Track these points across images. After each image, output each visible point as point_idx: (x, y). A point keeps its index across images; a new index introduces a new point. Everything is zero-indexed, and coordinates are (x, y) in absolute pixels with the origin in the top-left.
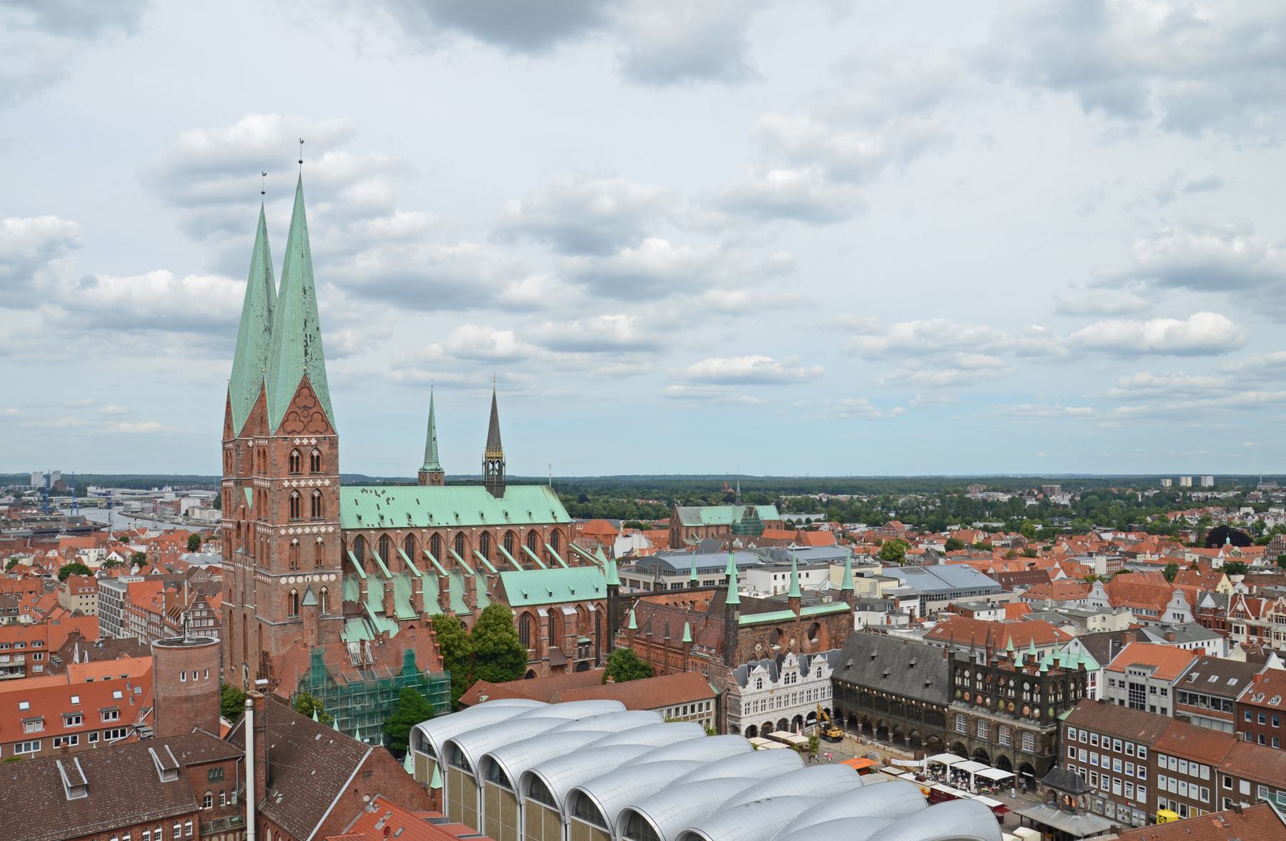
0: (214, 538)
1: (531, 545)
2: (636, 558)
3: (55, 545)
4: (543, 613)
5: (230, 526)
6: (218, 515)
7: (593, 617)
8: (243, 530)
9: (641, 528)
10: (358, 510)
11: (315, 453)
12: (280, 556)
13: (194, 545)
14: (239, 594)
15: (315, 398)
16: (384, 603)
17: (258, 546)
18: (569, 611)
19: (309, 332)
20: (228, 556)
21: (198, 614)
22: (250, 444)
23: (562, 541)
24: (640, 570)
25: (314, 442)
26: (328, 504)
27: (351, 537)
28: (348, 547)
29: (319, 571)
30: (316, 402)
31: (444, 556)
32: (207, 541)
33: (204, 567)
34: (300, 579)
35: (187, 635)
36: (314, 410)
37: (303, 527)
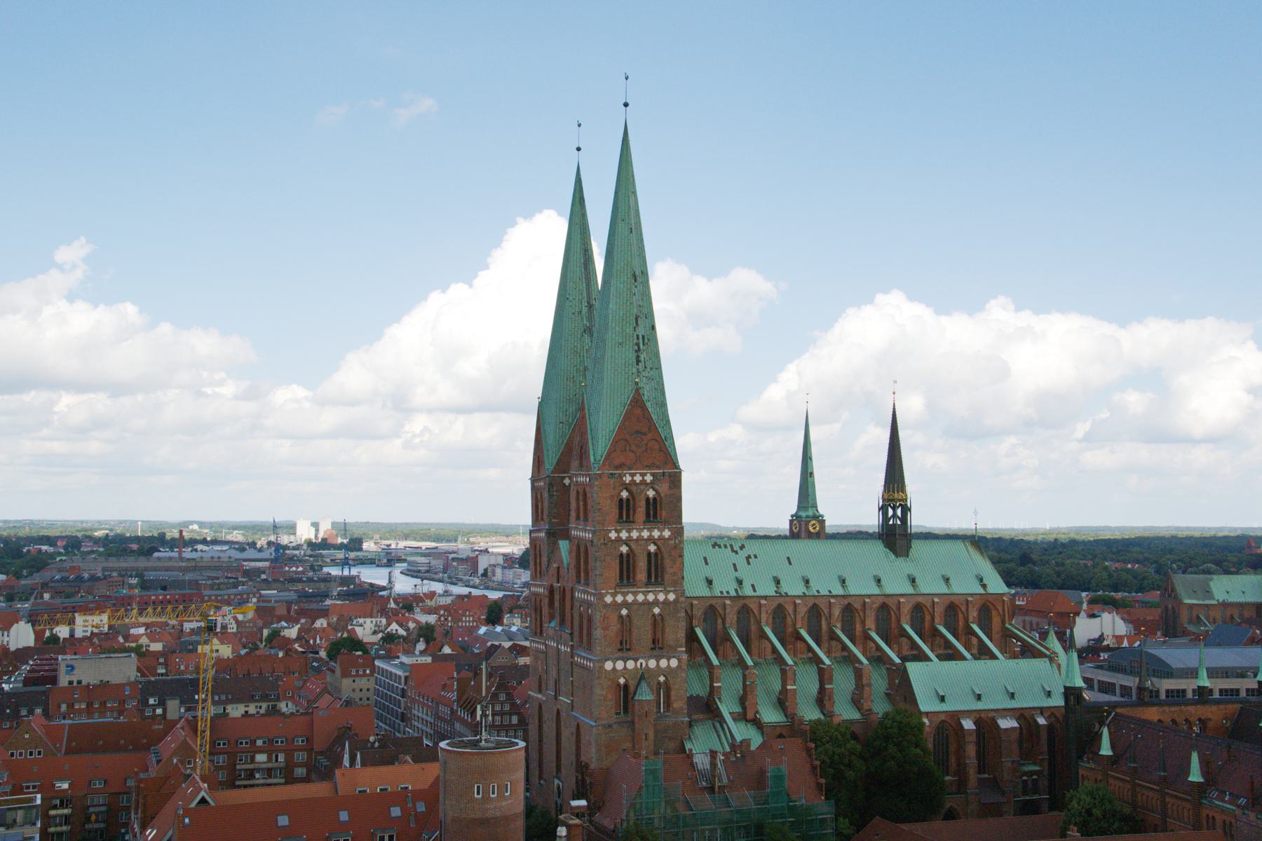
0: (521, 607)
1: (949, 626)
2: (1107, 649)
3: (324, 613)
4: (968, 724)
5: (541, 590)
6: (525, 576)
7: (1044, 735)
8: (557, 597)
9: (1114, 605)
10: (708, 572)
11: (651, 493)
13: (494, 614)
14: (551, 683)
16: (743, 700)
17: (576, 619)
19: (641, 331)
20: (538, 631)
21: (498, 708)
22: (567, 481)
23: (996, 621)
24: (1113, 668)
25: (649, 478)
26: (667, 563)
28: (695, 622)
29: (656, 652)
30: (652, 427)
31: (825, 637)
32: (511, 612)
33: (507, 644)
34: (631, 664)
35: (484, 735)
37: (635, 594)
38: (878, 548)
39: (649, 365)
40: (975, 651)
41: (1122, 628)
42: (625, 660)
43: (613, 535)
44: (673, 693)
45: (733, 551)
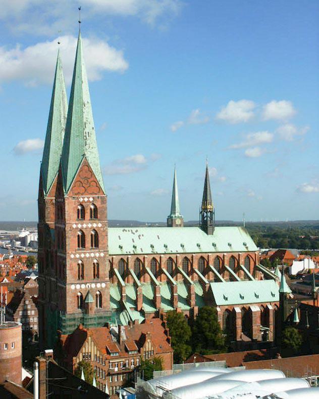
1: (230, 266)
12: (71, 273)
15: (91, 172)
18: (255, 309)
23: (252, 263)
25: (91, 199)
27: (116, 260)
28: (114, 266)
29: (95, 281)
34: (83, 286)
36: (92, 179)
37: (85, 253)
38: (198, 231)
39: (91, 147)
40: (243, 277)
41: (279, 266)
42: (80, 284)
43: (74, 226)
44: (103, 299)
45: (132, 233)
